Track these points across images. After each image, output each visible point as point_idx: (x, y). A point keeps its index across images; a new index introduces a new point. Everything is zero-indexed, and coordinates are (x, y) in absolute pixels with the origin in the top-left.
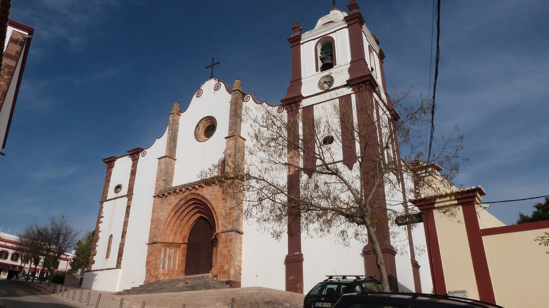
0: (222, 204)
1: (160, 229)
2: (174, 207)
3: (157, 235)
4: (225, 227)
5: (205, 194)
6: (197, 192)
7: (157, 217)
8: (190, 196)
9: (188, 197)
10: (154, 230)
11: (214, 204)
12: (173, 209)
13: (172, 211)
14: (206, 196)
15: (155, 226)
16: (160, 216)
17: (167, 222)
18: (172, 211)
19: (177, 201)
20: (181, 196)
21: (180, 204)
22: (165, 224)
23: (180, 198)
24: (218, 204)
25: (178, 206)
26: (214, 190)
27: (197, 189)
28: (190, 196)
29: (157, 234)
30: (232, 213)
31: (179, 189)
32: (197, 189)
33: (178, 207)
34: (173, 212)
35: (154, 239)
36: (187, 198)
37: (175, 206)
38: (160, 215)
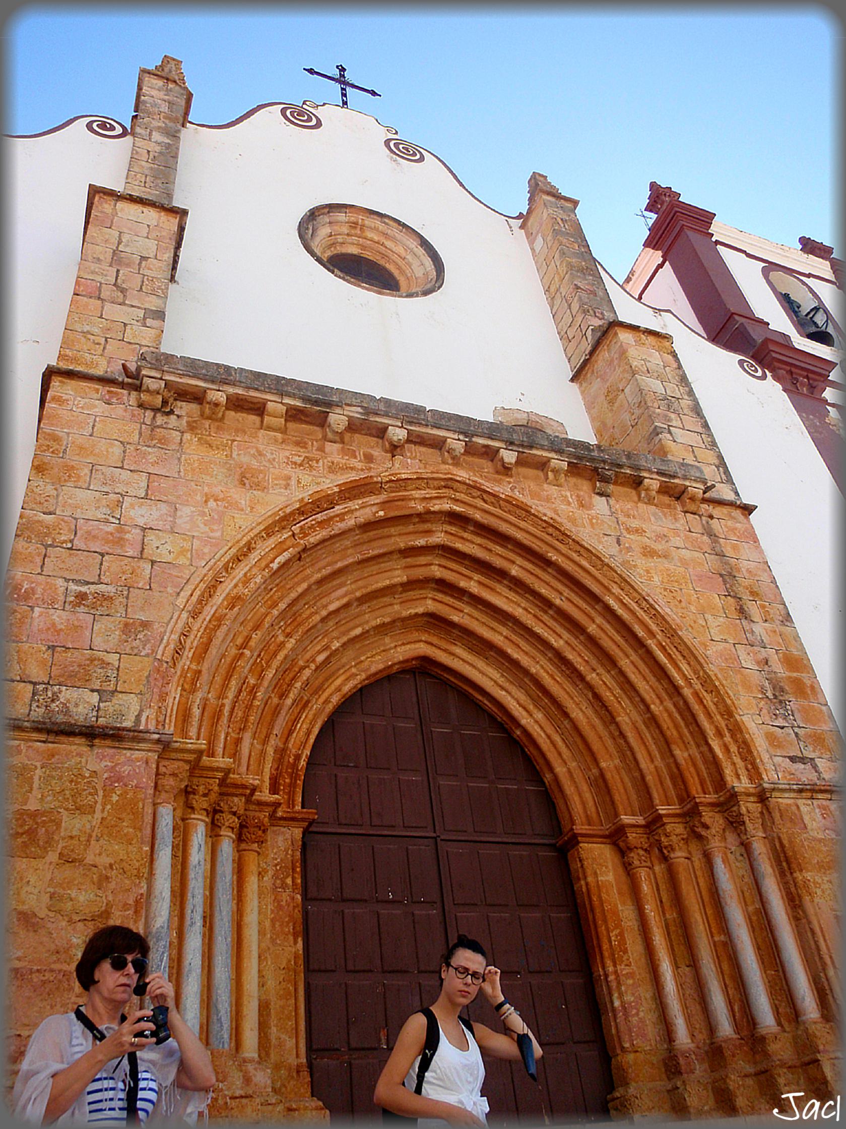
0: (721, 619)
1: (145, 625)
2: (292, 513)
3: (105, 664)
4: (802, 760)
5: (573, 521)
6: (503, 489)
7: (110, 528)
8: (434, 493)
9: (417, 494)
10: (59, 617)
11: (661, 602)
12: (284, 521)
13: (269, 532)
14: (586, 535)
15: (73, 587)
16: (144, 529)
17: (219, 598)
18: (269, 535)
19: (330, 484)
20: (354, 463)
21: (338, 509)
22: (202, 602)
23: (352, 476)
24: (693, 608)
25: (320, 517)
26: (635, 524)
27: (506, 470)
28: (434, 493)
29: (113, 658)
30: (812, 688)
31: (355, 412)
32: (506, 470)
33: (321, 524)
34: (280, 548)
35: (67, 694)
36: (403, 499)
37: (303, 511)
38: (141, 522)
